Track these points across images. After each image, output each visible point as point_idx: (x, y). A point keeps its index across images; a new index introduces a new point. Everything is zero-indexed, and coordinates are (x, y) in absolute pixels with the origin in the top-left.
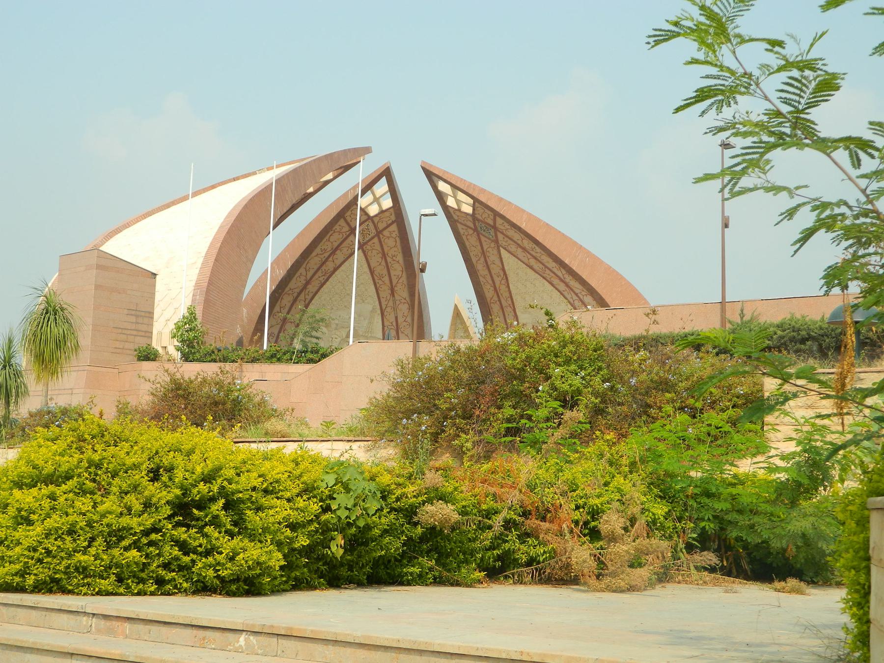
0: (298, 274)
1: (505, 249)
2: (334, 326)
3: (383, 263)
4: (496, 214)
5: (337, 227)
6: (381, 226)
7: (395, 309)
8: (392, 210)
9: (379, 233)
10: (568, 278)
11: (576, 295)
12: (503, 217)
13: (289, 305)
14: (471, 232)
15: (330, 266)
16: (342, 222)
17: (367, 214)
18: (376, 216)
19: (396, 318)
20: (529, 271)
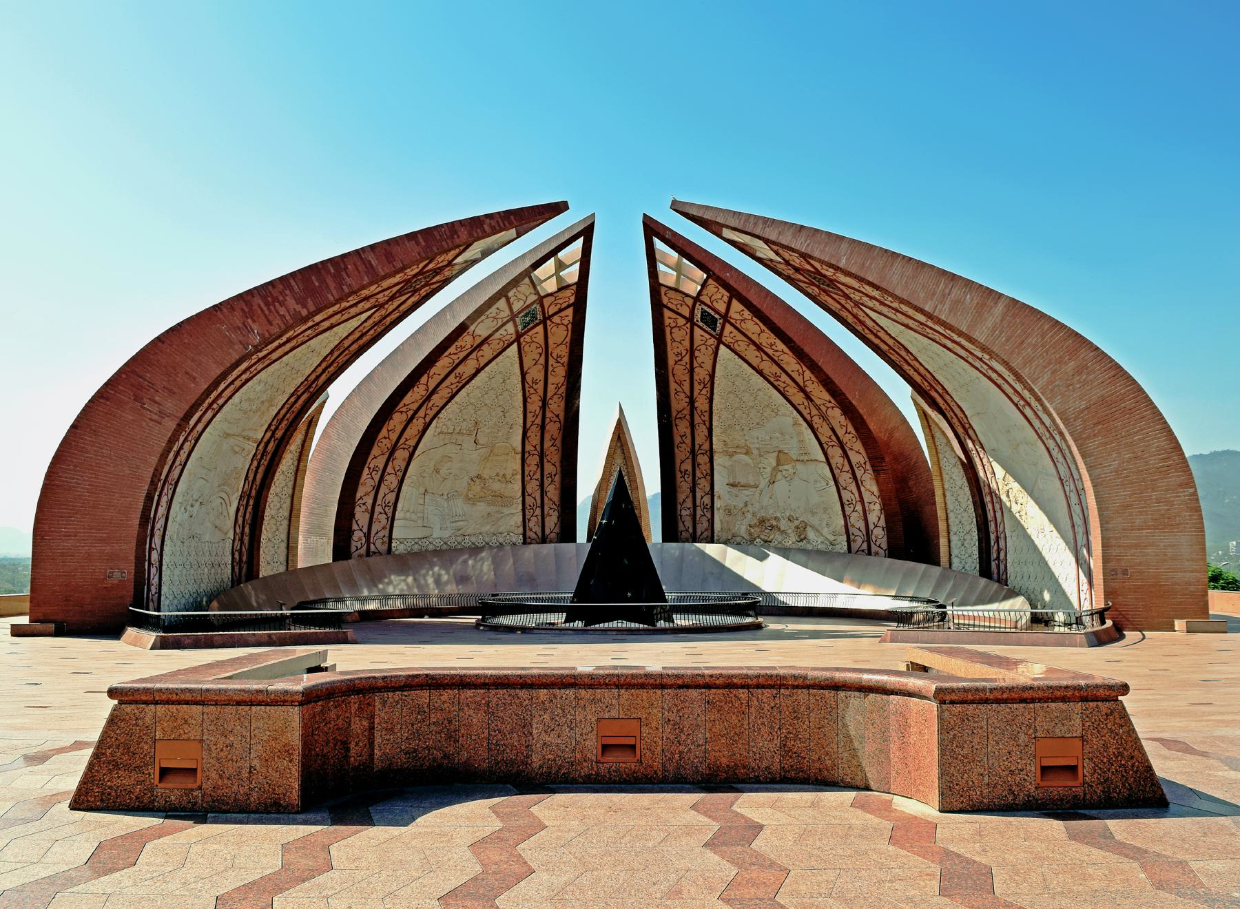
0: (672, 393)
2: (755, 452)
3: (765, 357)
4: (805, 256)
5: (667, 321)
7: (824, 417)
8: (710, 281)
9: (725, 317)
11: (981, 360)
12: (811, 257)
13: (688, 431)
15: (701, 374)
16: (667, 313)
17: (687, 295)
18: (700, 293)
19: (833, 430)
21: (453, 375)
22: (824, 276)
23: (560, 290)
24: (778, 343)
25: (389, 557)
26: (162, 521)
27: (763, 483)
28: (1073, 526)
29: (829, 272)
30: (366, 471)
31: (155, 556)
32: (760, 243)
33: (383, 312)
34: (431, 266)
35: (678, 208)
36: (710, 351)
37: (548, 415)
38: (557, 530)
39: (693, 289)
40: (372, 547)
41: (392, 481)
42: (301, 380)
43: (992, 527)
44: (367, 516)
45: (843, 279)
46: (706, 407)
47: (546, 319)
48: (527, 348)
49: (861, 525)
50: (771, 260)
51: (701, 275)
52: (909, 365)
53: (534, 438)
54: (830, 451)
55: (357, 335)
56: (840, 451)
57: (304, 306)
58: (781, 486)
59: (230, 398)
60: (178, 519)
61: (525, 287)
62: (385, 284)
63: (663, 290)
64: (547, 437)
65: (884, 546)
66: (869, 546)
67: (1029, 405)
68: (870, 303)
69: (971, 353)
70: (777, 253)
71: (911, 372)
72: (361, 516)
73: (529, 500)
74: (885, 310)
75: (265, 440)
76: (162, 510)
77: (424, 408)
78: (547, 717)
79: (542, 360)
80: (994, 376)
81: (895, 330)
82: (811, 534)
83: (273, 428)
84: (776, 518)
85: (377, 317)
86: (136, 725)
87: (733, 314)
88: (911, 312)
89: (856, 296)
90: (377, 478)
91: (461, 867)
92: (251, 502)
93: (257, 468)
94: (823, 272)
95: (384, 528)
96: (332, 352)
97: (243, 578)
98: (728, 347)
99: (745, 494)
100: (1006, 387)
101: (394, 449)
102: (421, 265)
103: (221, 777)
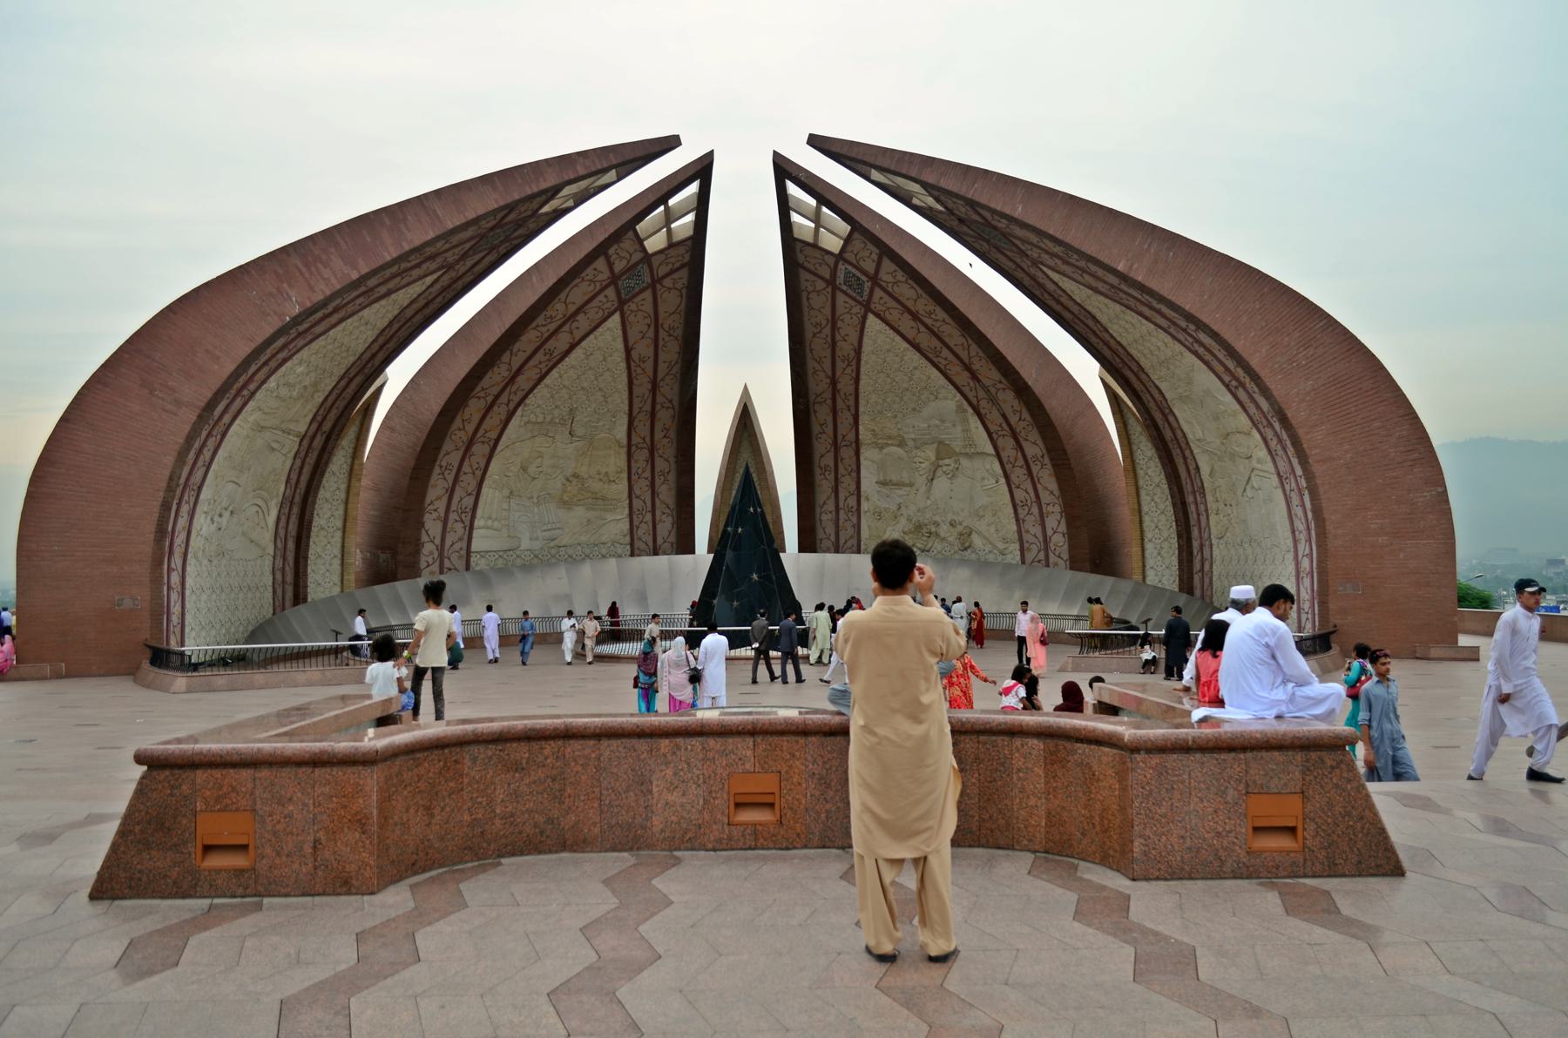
0: (810, 372)
2: (911, 443)
3: (922, 329)
4: (972, 204)
5: (804, 284)
6: (870, 266)
7: (993, 401)
8: (856, 235)
9: (875, 279)
10: (1154, 303)
11: (1185, 330)
12: (978, 204)
13: (830, 420)
15: (845, 349)
16: (804, 275)
19: (1004, 416)
20: (1101, 298)
21: (541, 352)
22: (995, 228)
23: (672, 245)
24: (939, 310)
25: (467, 575)
26: (183, 536)
27: (921, 481)
28: (1293, 532)
29: (1002, 224)
30: (437, 470)
31: (175, 578)
32: (915, 188)
33: (453, 274)
34: (512, 217)
35: (818, 142)
36: (856, 320)
37: (659, 399)
38: (673, 539)
39: (832, 243)
40: (447, 564)
41: (468, 481)
42: (352, 359)
43: (1195, 533)
44: (439, 525)
45: (1019, 232)
46: (851, 389)
48: (631, 318)
49: (1037, 530)
50: (931, 208)
51: (845, 228)
53: (643, 429)
54: (1000, 442)
55: (422, 302)
56: (1012, 442)
57: (354, 266)
58: (942, 484)
59: (264, 382)
60: (204, 532)
61: (627, 243)
62: (455, 240)
63: (799, 246)
64: (658, 426)
65: (1066, 556)
66: (1047, 556)
67: (1242, 385)
68: (1051, 262)
69: (1174, 324)
70: (937, 200)
71: (1100, 346)
72: (432, 525)
73: (637, 503)
74: (1068, 270)
75: (310, 433)
76: (182, 522)
77: (506, 393)
78: (669, 772)
79: (651, 334)
80: (1201, 350)
81: (1079, 293)
82: (977, 540)
83: (319, 418)
84: (937, 524)
85: (446, 280)
86: (171, 795)
87: (884, 276)
88: (1100, 272)
89: (1034, 254)
90: (450, 478)
91: (570, 958)
92: (296, 510)
93: (301, 468)
95: (460, 539)
96: (391, 323)
97: (288, 603)
98: (878, 316)
100: (1215, 363)
102: (499, 217)
103: (278, 854)
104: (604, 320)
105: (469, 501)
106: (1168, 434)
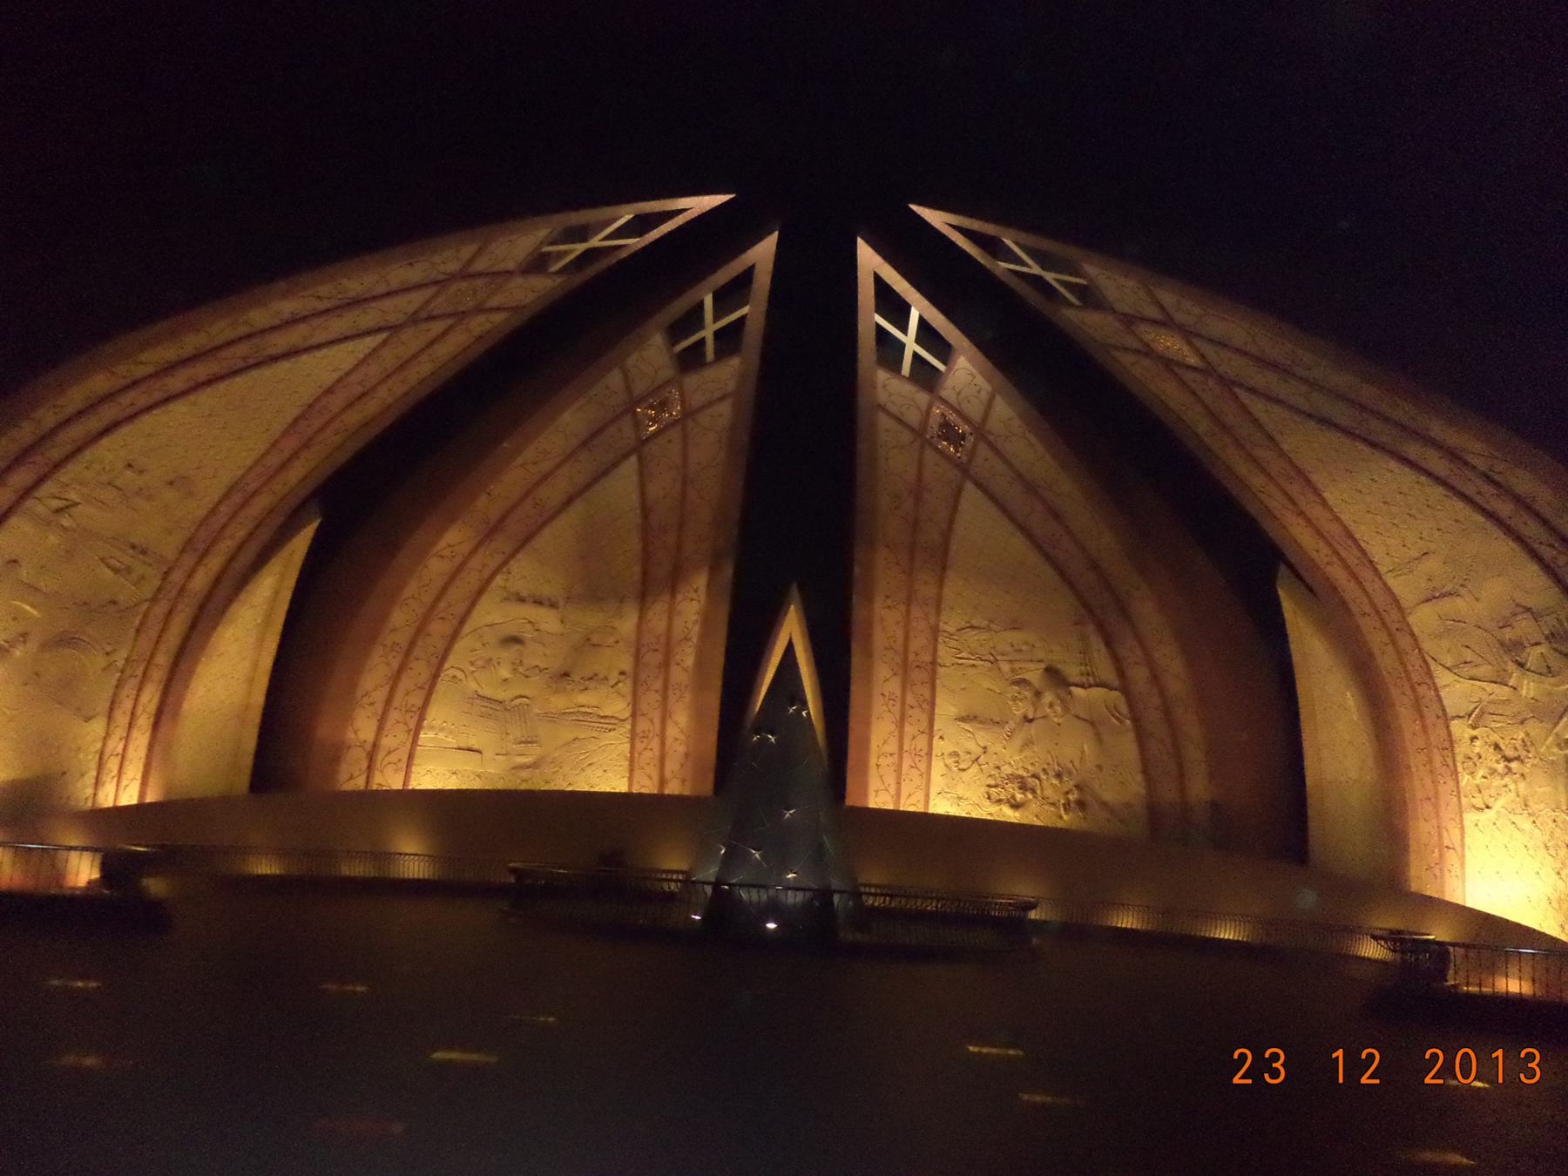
1: (1241, 385)
6: (974, 410)
9: (980, 431)
14: (1146, 362)
41: (419, 671)
44: (374, 725)
47: (689, 414)
52: (1301, 514)
74: (1283, 389)
80: (1505, 508)
83: (201, 547)
85: (389, 358)
89: (1231, 365)
90: (396, 664)
92: (158, 675)
94: (1179, 317)
98: (978, 485)
99: (983, 737)
101: (425, 620)
104: (615, 464)
105: (416, 700)
106: (1386, 661)
